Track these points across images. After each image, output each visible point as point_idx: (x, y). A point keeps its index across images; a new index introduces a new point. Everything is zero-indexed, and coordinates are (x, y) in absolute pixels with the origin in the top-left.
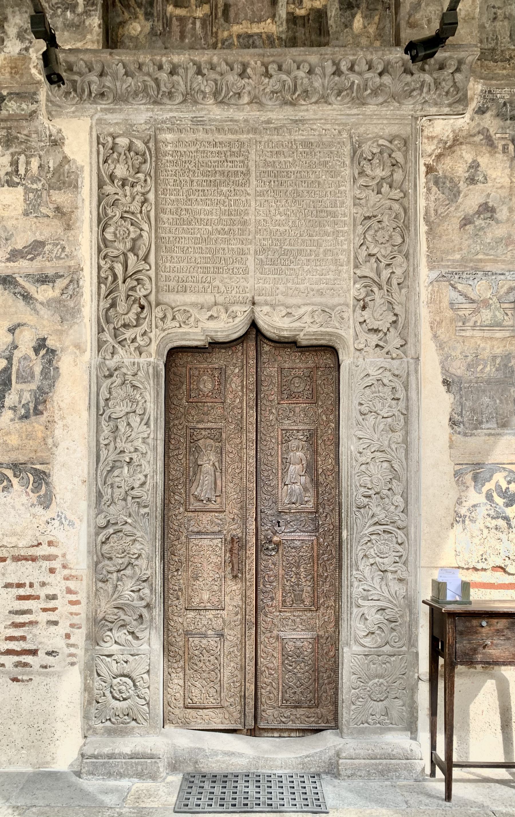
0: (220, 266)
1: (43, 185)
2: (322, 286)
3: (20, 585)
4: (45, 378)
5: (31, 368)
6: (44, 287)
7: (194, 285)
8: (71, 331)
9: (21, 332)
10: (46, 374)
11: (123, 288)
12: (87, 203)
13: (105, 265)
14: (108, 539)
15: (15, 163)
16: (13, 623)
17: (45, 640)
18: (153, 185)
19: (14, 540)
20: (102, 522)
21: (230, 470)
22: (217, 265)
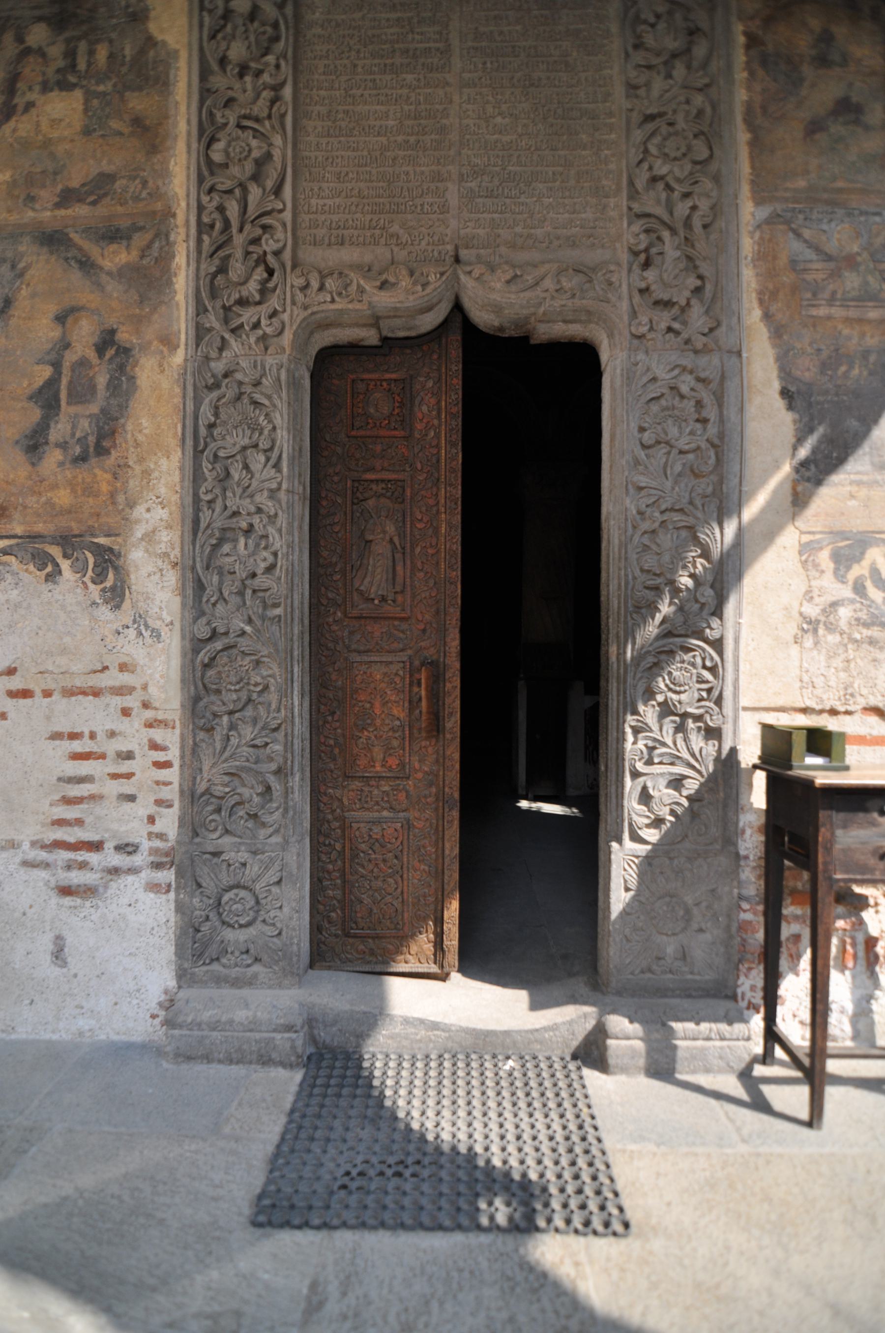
0: (401, 200)
1: (115, 85)
2: (575, 230)
3: (74, 736)
4: (113, 395)
5: (92, 379)
6: (114, 247)
7: (356, 233)
8: (156, 316)
9: (76, 321)
10: (115, 388)
11: (239, 240)
12: (183, 108)
13: (211, 203)
14: (213, 659)
15: (71, 54)
16: (64, 797)
17: (115, 826)
18: (290, 72)
19: (62, 661)
20: (203, 632)
21: (418, 550)
22: (396, 200)
